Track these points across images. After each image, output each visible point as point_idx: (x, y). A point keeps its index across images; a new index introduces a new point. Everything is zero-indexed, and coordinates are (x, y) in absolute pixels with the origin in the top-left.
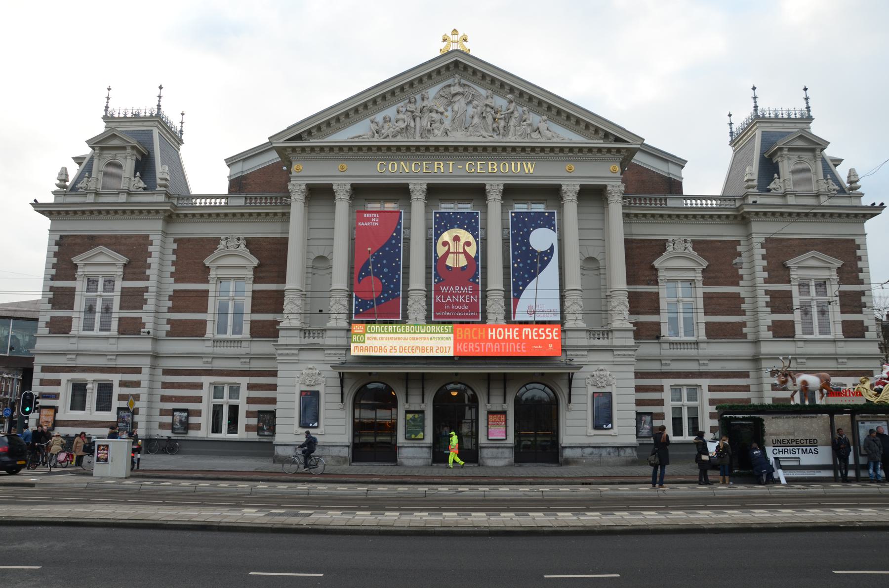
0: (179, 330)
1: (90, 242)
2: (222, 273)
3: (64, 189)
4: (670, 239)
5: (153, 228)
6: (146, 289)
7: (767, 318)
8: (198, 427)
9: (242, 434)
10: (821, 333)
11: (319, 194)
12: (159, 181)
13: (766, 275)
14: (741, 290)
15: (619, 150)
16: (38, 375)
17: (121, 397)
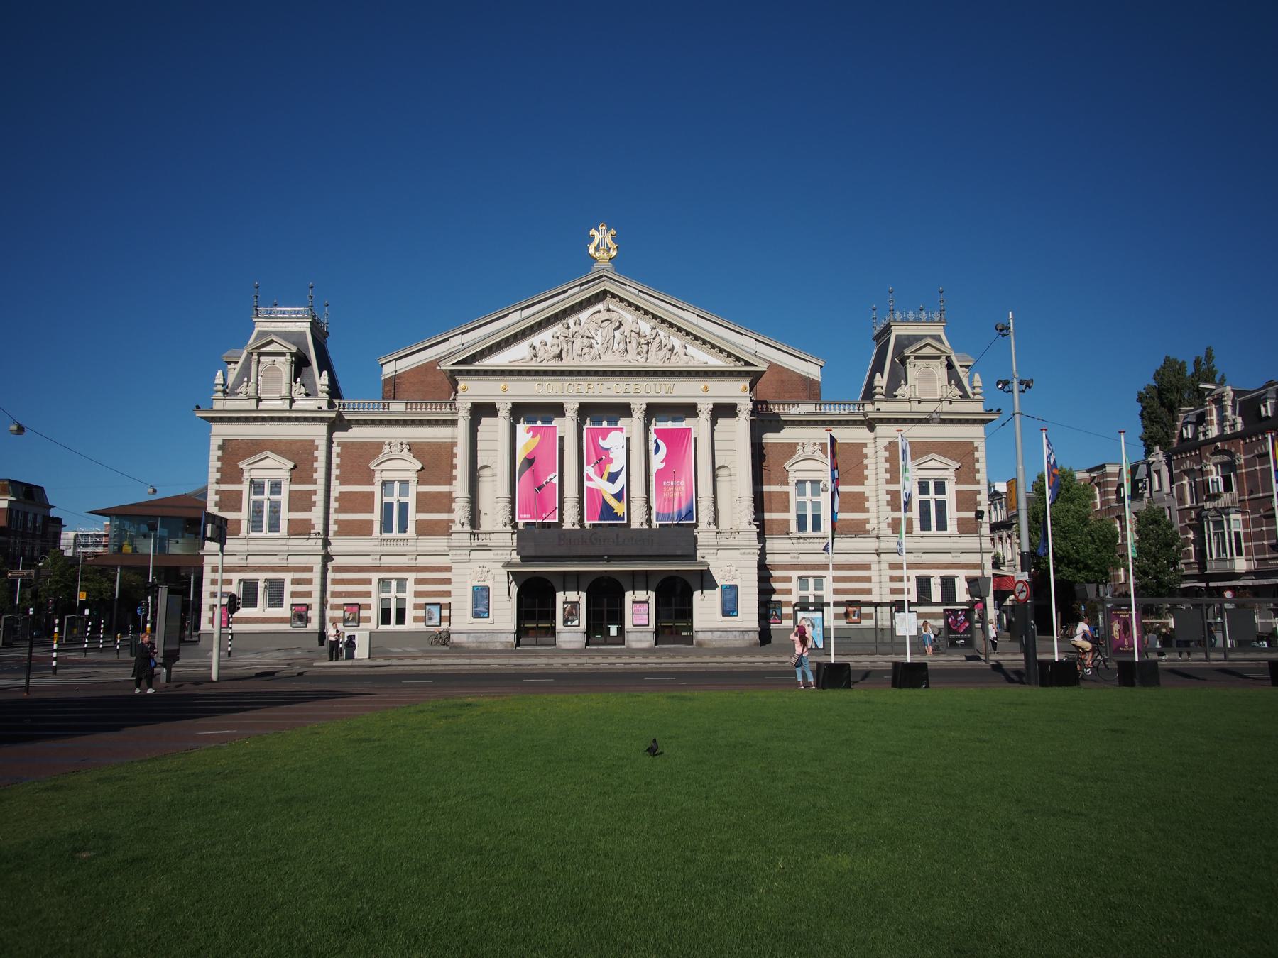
0: (349, 530)
1: (255, 448)
2: (388, 476)
5: (318, 432)
6: (314, 492)
8: (368, 620)
10: (938, 528)
11: (482, 410)
12: (319, 386)
14: (868, 489)
15: (747, 374)
16: (208, 576)
17: (294, 594)
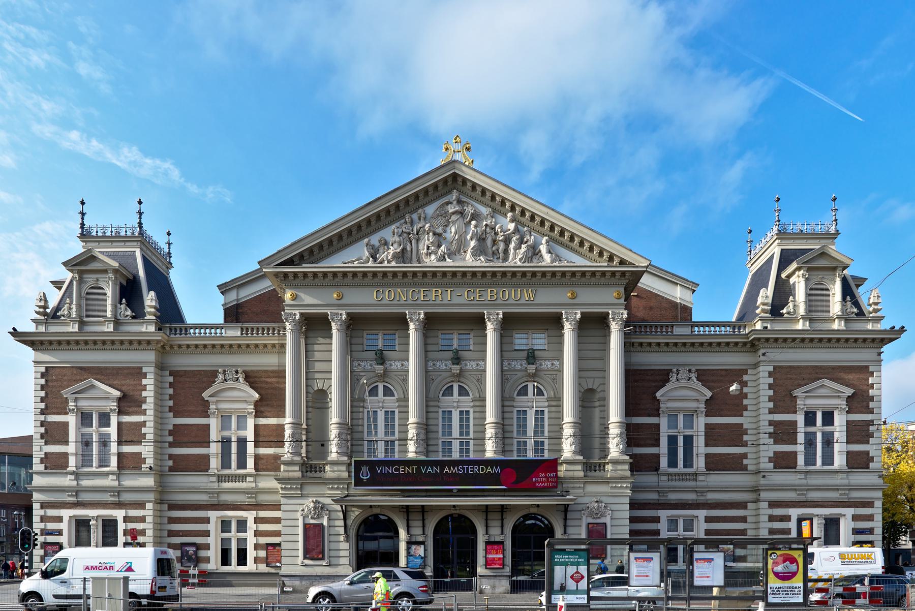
3: (50, 316)
4: (675, 370)
7: (769, 448)
9: (251, 566)
13: (771, 405)
